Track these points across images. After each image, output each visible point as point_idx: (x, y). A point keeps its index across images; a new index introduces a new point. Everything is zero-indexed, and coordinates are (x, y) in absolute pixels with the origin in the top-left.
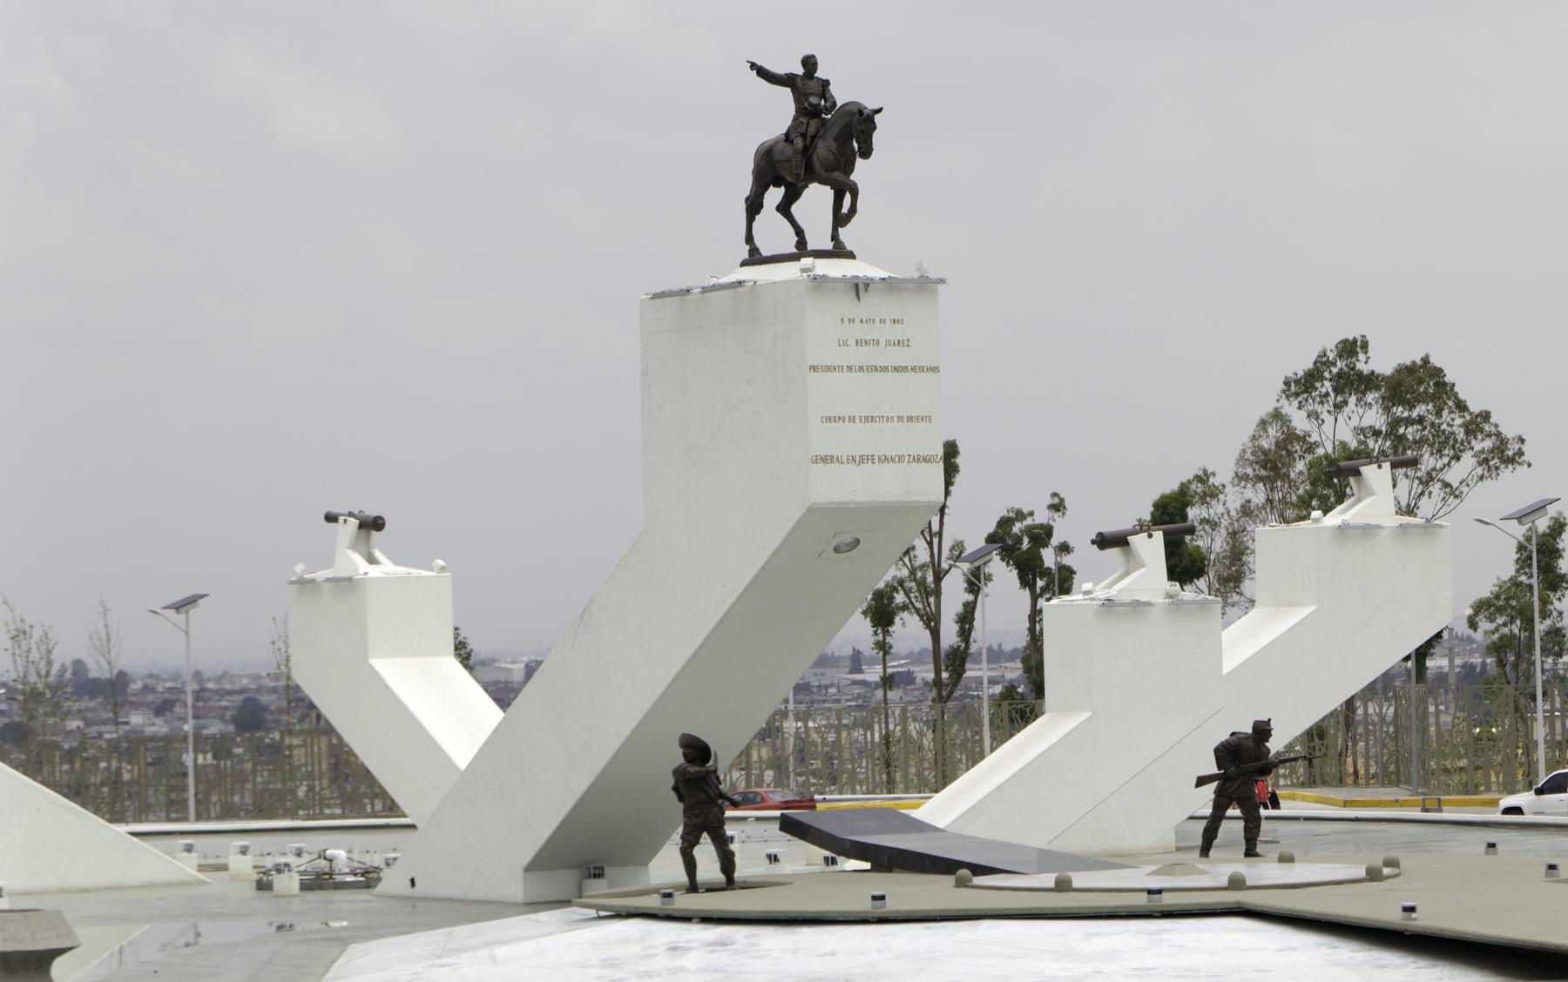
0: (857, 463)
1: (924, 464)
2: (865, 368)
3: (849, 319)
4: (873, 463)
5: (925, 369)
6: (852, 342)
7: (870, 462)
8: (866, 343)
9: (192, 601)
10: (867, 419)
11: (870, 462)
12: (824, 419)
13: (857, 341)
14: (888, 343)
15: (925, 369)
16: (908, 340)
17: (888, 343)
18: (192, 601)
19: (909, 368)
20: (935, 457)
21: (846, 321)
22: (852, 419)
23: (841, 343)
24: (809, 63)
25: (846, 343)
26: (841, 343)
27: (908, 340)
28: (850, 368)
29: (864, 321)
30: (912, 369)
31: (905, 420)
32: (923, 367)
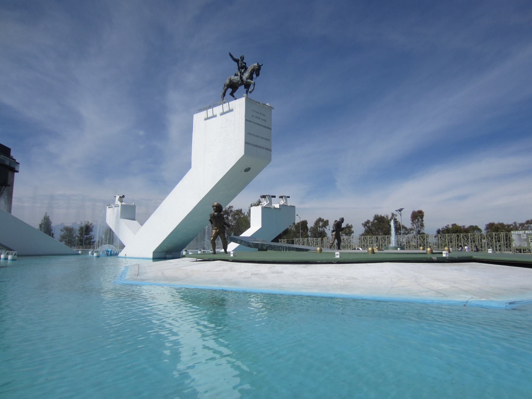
14: (262, 119)
17: (262, 119)
24: (242, 58)
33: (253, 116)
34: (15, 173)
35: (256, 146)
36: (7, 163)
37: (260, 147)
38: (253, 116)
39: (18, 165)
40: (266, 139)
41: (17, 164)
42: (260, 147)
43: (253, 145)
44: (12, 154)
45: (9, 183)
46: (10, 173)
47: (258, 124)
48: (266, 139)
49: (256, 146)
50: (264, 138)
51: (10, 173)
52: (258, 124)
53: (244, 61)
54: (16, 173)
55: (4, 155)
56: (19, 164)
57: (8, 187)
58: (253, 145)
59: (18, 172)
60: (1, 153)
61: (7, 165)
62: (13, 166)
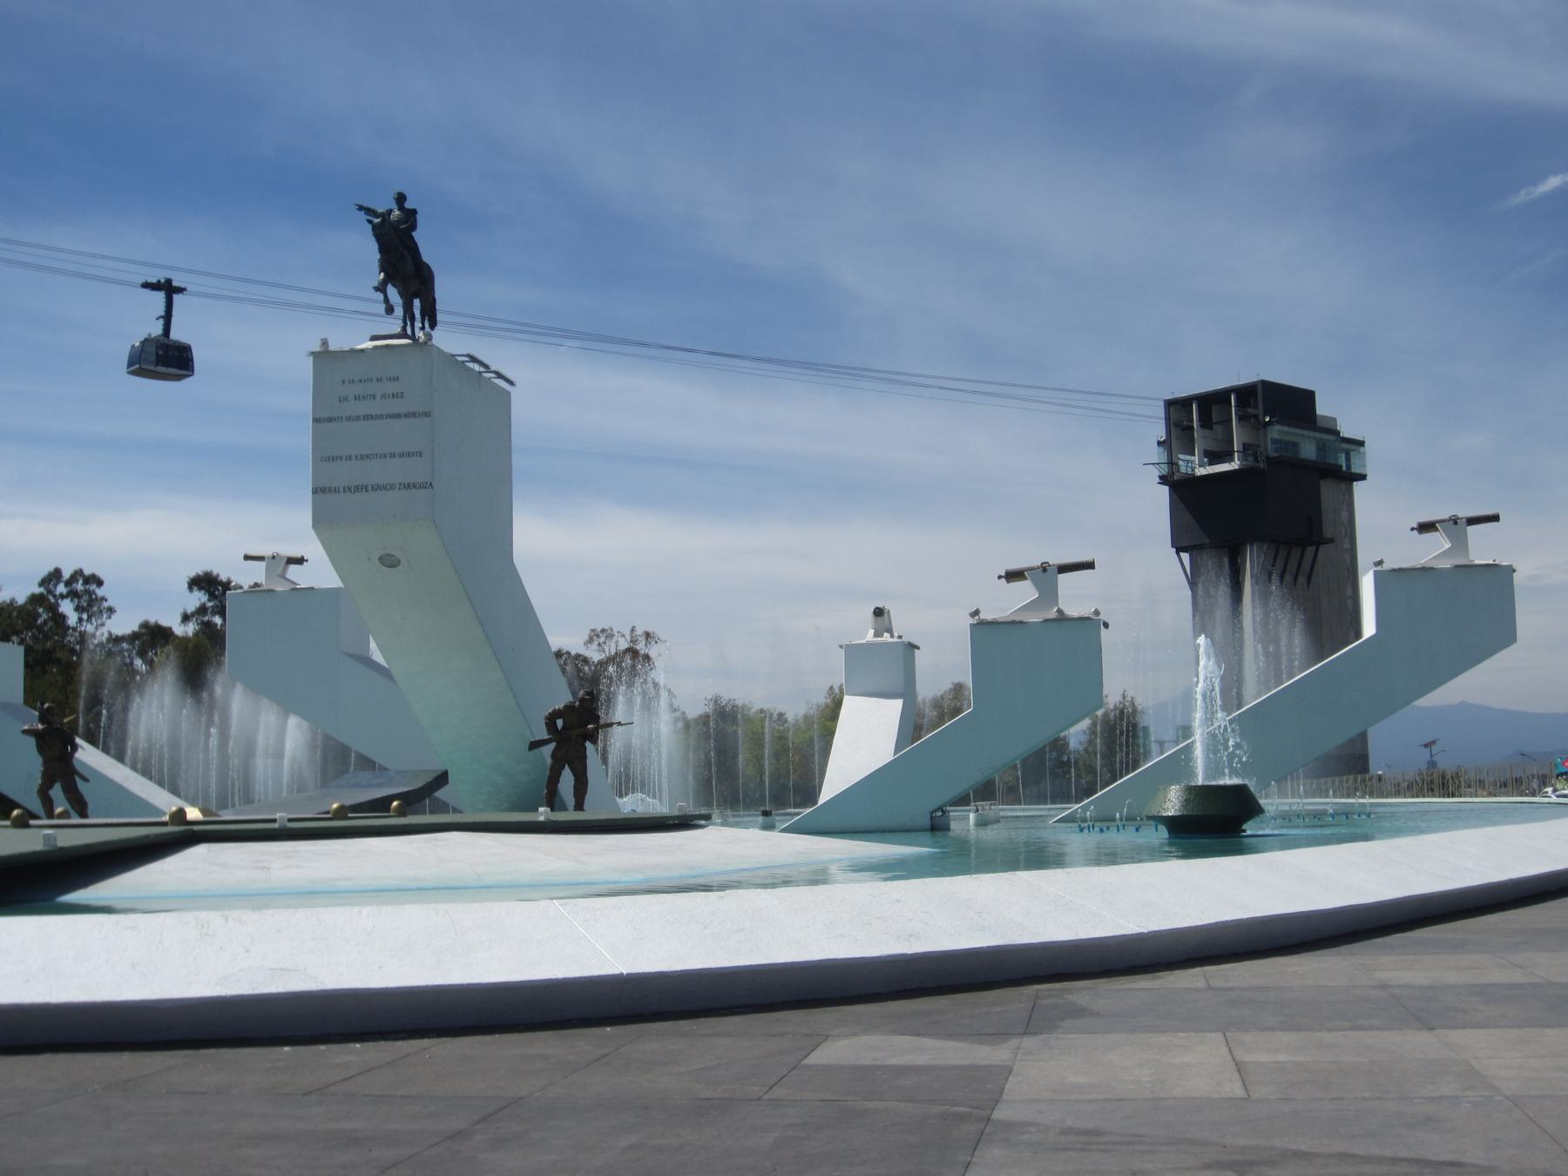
0: (353, 490)
6: (351, 398)
7: (364, 490)
8: (363, 397)
9: (1433, 742)
11: (364, 490)
13: (355, 397)
14: (384, 396)
17: (384, 396)
18: (1433, 742)
22: (349, 458)
23: (342, 399)
25: (345, 399)
26: (342, 399)
27: (402, 393)
28: (349, 418)
30: (405, 416)
32: (415, 413)
33: (345, 399)
34: (1355, 483)
35: (360, 488)
36: (1308, 451)
37: (376, 488)
38: (343, 399)
39: (1362, 449)
40: (402, 455)
41: (1354, 447)
42: (376, 488)
43: (348, 489)
44: (1322, 409)
45: (1328, 531)
46: (1328, 490)
47: (367, 417)
48: (402, 455)
49: (360, 488)
50: (393, 455)
51: (1328, 490)
52: (367, 417)
53: (408, 205)
54: (1358, 487)
55: (1288, 425)
56: (1362, 443)
57: (1325, 546)
58: (348, 489)
59: (1363, 477)
60: (1275, 419)
61: (1310, 461)
62: (1333, 462)
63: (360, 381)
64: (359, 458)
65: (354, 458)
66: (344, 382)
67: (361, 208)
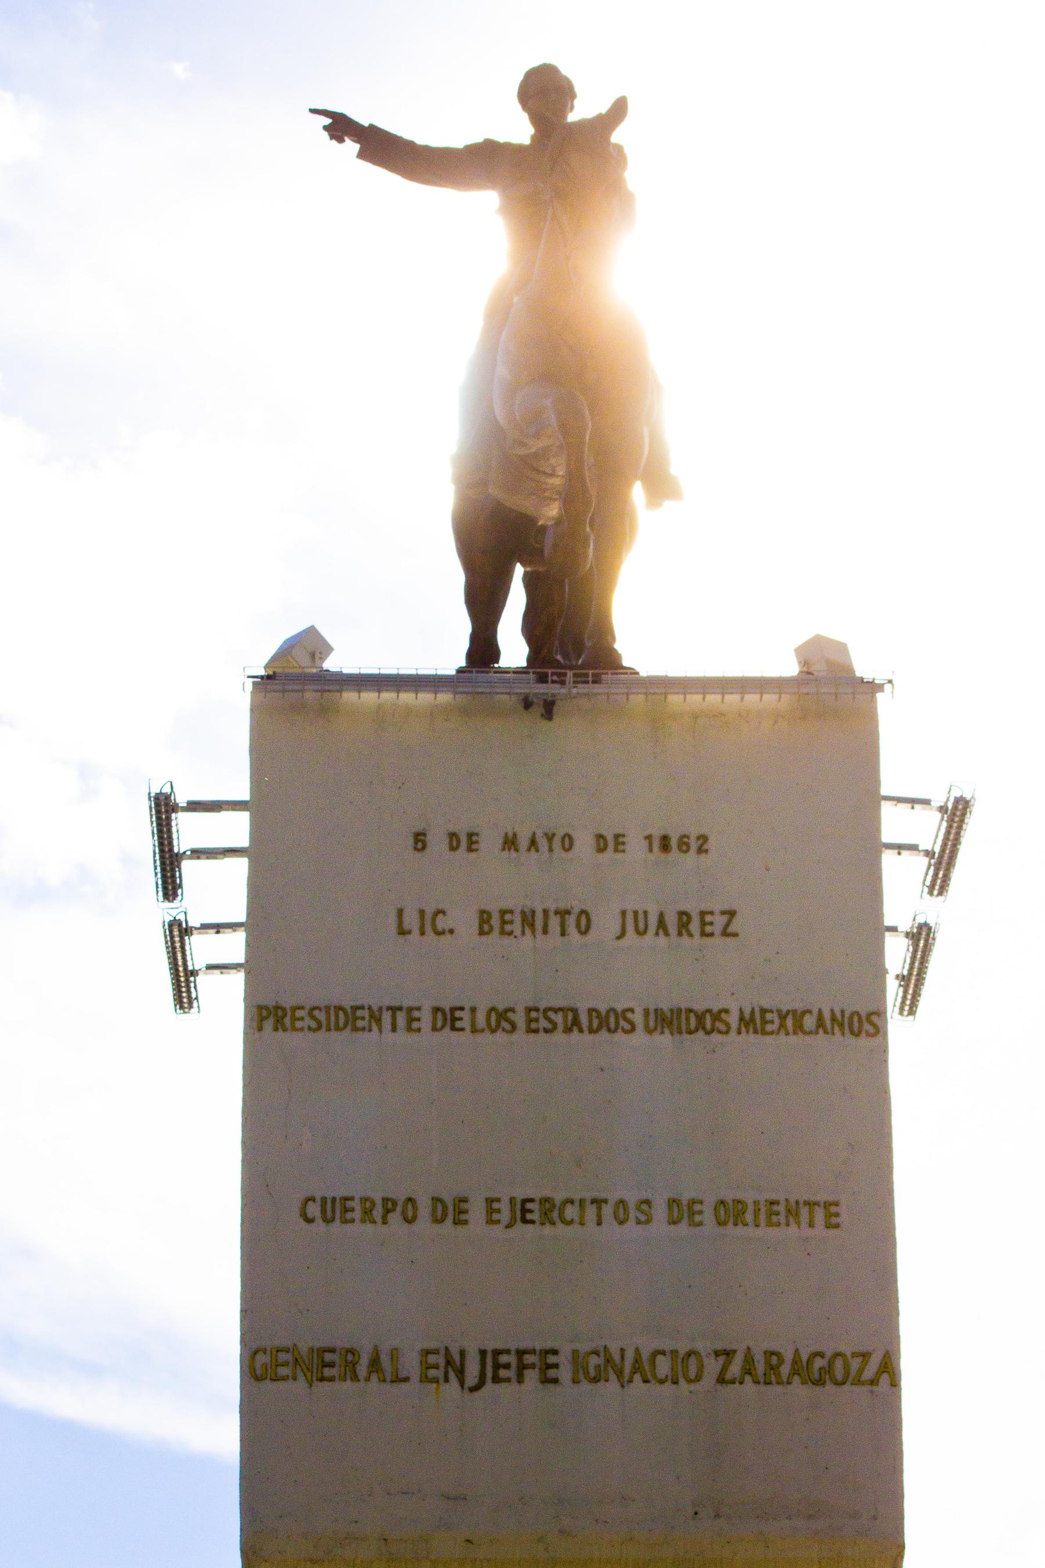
1: (800, 1391)
2: (520, 1019)
3: (453, 835)
4: (546, 1380)
5: (809, 1022)
7: (532, 1376)
10: (522, 1211)
11: (532, 1376)
12: (313, 1210)
13: (484, 917)
15: (809, 1022)
16: (731, 914)
19: (733, 1019)
20: (855, 1364)
21: (437, 842)
23: (411, 920)
26: (411, 920)
27: (731, 914)
29: (524, 843)
31: (708, 1217)
32: (798, 1016)
63: (510, 843)
64: (505, 1216)
65: (476, 1211)
66: (420, 840)
67: (313, 111)
